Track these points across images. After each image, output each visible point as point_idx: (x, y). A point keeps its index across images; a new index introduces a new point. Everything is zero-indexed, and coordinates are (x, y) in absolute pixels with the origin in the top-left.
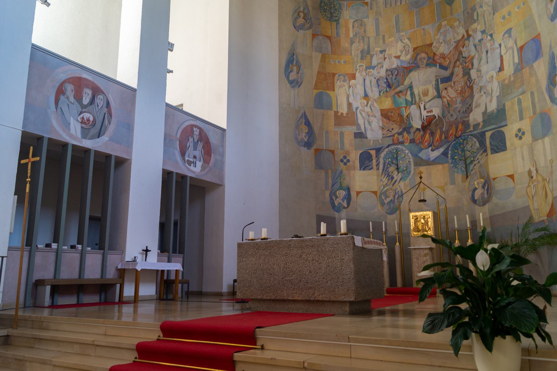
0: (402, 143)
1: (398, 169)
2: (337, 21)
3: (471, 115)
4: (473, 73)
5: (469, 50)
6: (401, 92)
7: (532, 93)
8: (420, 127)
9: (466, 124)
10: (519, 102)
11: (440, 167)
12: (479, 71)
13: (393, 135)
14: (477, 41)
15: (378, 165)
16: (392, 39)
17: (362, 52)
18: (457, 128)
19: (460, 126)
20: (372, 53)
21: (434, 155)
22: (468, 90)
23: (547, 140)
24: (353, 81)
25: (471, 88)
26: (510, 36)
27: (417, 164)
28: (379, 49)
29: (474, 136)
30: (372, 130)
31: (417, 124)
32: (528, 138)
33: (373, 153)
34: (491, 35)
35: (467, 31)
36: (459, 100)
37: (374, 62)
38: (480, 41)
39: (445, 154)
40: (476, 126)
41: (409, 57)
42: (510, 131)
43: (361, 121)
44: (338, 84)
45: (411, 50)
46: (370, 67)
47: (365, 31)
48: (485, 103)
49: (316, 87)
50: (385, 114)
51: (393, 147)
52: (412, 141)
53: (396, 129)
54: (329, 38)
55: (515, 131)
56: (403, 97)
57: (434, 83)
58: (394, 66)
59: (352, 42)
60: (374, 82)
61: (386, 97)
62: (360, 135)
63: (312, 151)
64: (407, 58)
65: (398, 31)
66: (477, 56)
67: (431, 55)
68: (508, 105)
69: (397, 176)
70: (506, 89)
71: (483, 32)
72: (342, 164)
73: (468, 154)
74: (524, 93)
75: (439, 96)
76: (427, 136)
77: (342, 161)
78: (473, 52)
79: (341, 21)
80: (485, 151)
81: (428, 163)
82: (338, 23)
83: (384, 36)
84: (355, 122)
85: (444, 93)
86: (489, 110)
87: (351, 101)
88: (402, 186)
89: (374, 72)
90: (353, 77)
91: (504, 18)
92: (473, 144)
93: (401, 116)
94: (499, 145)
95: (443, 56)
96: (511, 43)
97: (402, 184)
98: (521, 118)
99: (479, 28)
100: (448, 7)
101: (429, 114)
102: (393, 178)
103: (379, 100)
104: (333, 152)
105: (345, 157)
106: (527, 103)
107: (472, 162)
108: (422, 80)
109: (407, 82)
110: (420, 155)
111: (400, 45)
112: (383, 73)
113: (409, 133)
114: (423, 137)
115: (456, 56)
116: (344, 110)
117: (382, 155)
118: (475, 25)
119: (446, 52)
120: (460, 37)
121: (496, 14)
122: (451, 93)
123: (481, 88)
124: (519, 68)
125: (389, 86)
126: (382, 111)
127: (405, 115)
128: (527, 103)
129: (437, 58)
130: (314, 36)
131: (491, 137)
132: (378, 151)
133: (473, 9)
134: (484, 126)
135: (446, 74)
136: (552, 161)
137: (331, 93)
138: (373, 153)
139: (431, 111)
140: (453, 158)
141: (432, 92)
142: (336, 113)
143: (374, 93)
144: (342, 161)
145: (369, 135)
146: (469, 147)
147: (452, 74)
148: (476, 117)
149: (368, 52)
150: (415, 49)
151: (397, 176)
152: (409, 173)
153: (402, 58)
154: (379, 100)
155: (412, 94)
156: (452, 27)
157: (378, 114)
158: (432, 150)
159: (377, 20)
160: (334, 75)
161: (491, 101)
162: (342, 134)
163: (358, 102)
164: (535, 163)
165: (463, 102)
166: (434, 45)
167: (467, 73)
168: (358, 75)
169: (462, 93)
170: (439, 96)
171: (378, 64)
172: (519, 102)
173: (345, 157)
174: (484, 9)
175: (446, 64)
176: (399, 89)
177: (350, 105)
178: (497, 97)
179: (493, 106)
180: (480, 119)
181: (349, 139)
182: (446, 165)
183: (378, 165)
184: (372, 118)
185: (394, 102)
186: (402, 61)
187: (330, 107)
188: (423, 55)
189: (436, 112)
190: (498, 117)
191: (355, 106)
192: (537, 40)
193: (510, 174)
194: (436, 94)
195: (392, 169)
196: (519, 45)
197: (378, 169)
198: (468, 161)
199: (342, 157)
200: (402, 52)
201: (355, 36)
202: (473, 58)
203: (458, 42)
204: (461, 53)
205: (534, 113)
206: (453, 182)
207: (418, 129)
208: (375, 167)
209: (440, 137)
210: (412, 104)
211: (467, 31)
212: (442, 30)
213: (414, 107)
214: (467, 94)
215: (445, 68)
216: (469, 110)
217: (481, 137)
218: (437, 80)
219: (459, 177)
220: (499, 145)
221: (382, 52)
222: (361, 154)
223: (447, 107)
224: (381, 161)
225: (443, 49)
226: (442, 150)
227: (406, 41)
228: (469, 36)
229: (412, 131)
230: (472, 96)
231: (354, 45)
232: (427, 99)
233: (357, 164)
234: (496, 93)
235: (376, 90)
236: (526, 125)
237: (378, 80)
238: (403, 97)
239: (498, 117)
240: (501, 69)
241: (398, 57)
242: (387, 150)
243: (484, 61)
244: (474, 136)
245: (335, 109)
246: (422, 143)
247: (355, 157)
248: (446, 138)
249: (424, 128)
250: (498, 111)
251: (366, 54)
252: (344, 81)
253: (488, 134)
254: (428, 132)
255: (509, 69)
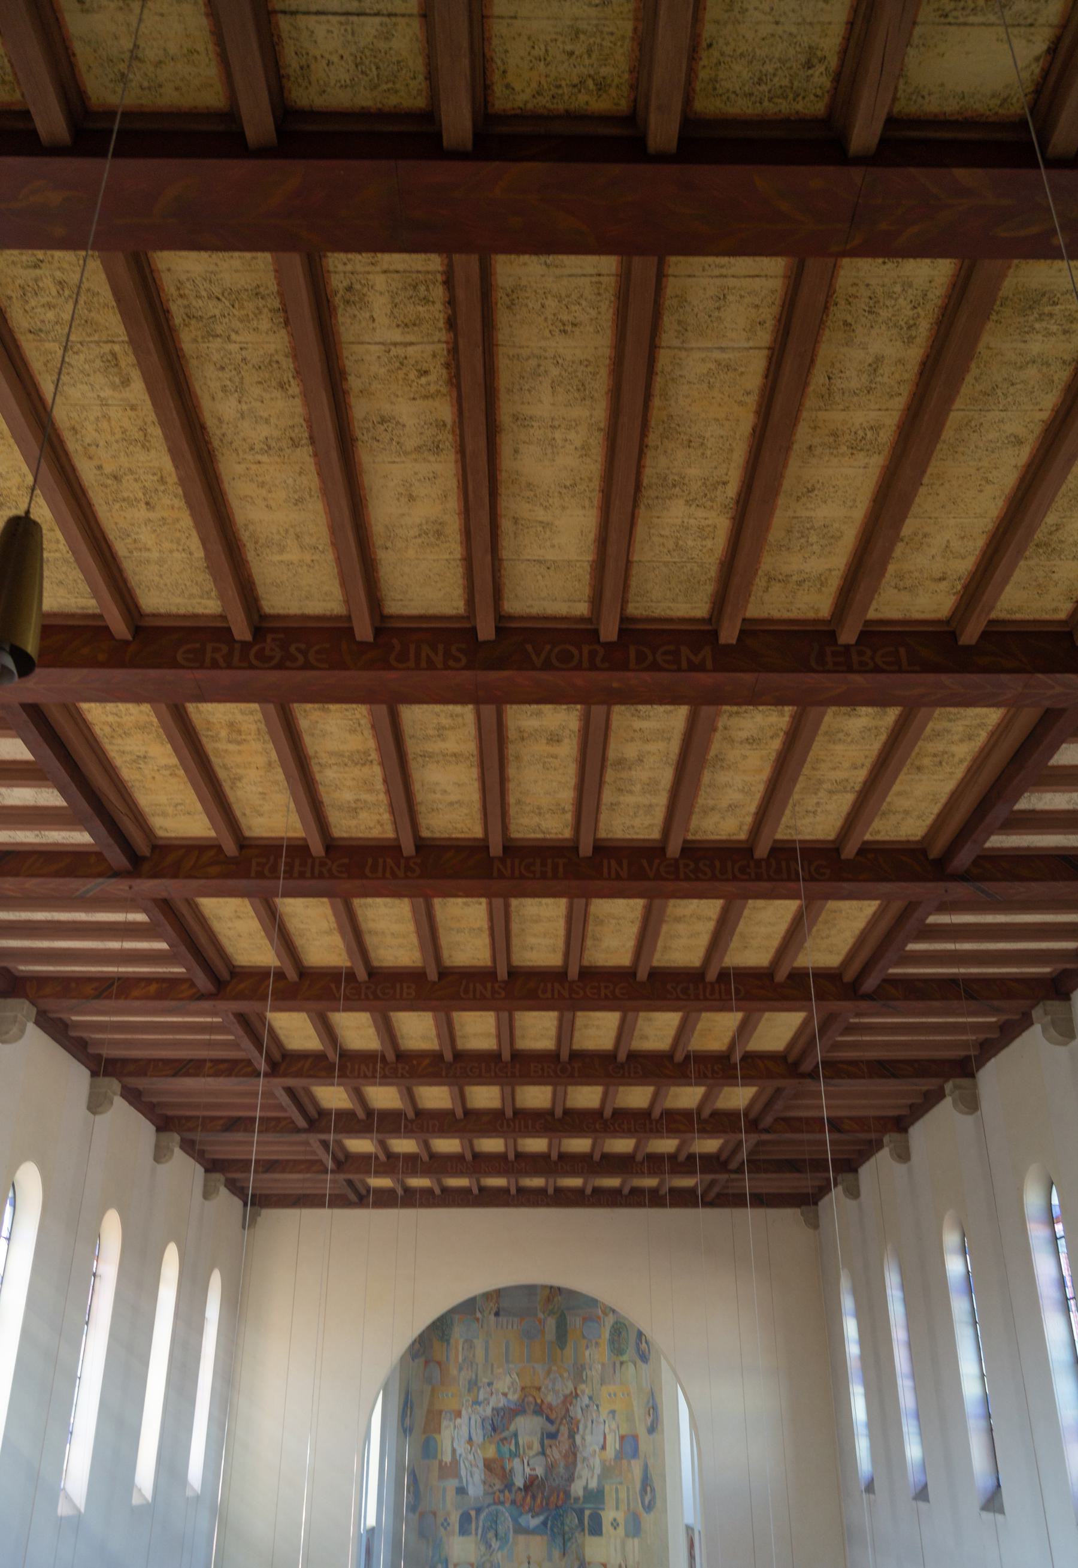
0: (502, 1503)
1: (496, 1535)
2: (448, 1341)
3: (573, 1486)
4: (578, 1438)
5: (576, 1412)
6: (506, 1439)
7: (628, 1488)
8: (521, 1486)
9: (567, 1494)
10: (617, 1491)
11: (538, 1538)
12: (583, 1438)
13: (494, 1493)
14: (584, 1406)
15: (477, 1529)
16: (501, 1370)
17: (470, 1382)
18: (558, 1496)
19: (561, 1494)
20: (479, 1384)
21: (534, 1522)
22: (572, 1455)
23: (636, 1541)
24: (458, 1421)
25: (575, 1455)
26: (614, 1418)
27: (516, 1532)
28: (486, 1380)
29: (574, 1510)
30: (474, 1484)
31: (519, 1482)
32: (621, 1530)
33: (473, 1513)
34: (597, 1406)
35: (576, 1389)
36: (562, 1464)
37: (481, 1397)
38: (587, 1406)
39: (544, 1523)
40: (577, 1499)
41: (516, 1397)
42: (608, 1515)
43: (463, 1473)
44: (444, 1423)
45: (519, 1389)
46: (476, 1402)
47: (474, 1356)
48: (586, 1479)
49: (424, 1432)
50: (488, 1465)
51: (493, 1507)
52: (513, 1502)
53: (498, 1486)
54: (439, 1363)
55: (611, 1519)
56: (507, 1445)
57: (539, 1435)
58: (501, 1405)
59: (461, 1369)
60: (479, 1420)
61: (490, 1443)
62: (461, 1491)
63: (417, 1514)
64: (514, 1397)
65: (507, 1361)
66: (582, 1422)
67: (539, 1401)
68: (607, 1488)
69: (495, 1544)
70: (607, 1471)
71: (590, 1398)
72: (442, 1529)
73: (567, 1528)
74: (621, 1483)
75: (543, 1453)
76: (529, 1498)
77: (442, 1525)
78: (579, 1415)
79: (452, 1341)
80: (583, 1530)
81: (527, 1531)
82: (448, 1344)
83: (492, 1365)
84: (457, 1475)
85: (548, 1452)
86: (590, 1486)
87: (455, 1446)
88: (499, 1556)
89: (480, 1409)
90: (459, 1414)
91: (610, 1395)
92: (572, 1520)
93: (503, 1468)
94: (596, 1529)
95: (550, 1407)
96: (614, 1426)
97: (499, 1555)
98: (617, 1508)
99: (587, 1391)
100: (559, 1351)
101: (533, 1473)
102: (490, 1546)
103: (482, 1447)
104: (435, 1514)
105: (446, 1520)
106: (623, 1495)
107: (570, 1539)
108: (528, 1428)
109: (512, 1428)
110: (520, 1520)
111: (508, 1380)
112: (489, 1412)
113: (510, 1491)
114: (524, 1499)
115: (563, 1412)
116: (447, 1458)
117: (482, 1516)
118: (583, 1386)
119: (554, 1403)
120: (567, 1392)
121: (604, 1387)
122: (555, 1454)
123: (584, 1459)
124: (620, 1455)
125: (494, 1429)
126: (485, 1460)
127: (508, 1468)
128: (623, 1495)
129: (544, 1407)
130: (427, 1363)
131: (591, 1516)
132: (478, 1511)
133: (583, 1367)
134: (584, 1502)
135: (552, 1429)
136: (638, 1563)
137: (436, 1436)
138: (473, 1513)
139: (534, 1469)
140: (552, 1530)
141: (537, 1447)
142: (441, 1462)
143: (478, 1438)
144: (442, 1525)
145: (471, 1491)
146: (568, 1521)
147: (558, 1431)
148: (577, 1489)
149: (476, 1383)
150: (523, 1389)
151: (495, 1544)
152: (507, 1542)
153: (510, 1396)
154: (482, 1447)
155: (517, 1444)
156: (561, 1376)
157: (481, 1464)
158: (533, 1517)
159: (487, 1342)
160: (441, 1412)
161: (592, 1477)
162: (444, 1490)
163: (461, 1448)
164: (625, 1559)
165: (567, 1467)
166: (543, 1389)
167: (572, 1436)
168: (464, 1412)
169: (566, 1456)
170: (543, 1453)
171: (485, 1399)
172: (617, 1491)
173: (446, 1520)
174: (594, 1373)
175: (553, 1416)
176: (506, 1434)
177: (454, 1451)
178: (599, 1476)
179: (593, 1484)
180: (581, 1493)
181: (451, 1494)
182: (545, 1538)
183: (477, 1529)
184: (475, 1469)
185: (499, 1450)
186: (509, 1401)
187: (435, 1457)
188: (531, 1399)
189: (540, 1471)
190: (596, 1497)
191: (458, 1452)
192: (635, 1438)
193: (603, 1561)
194: (540, 1449)
195: (490, 1534)
196: (622, 1432)
197: (476, 1534)
198: (566, 1537)
199: (442, 1520)
200: (509, 1389)
201: (464, 1360)
202: (578, 1422)
203: (566, 1397)
204: (568, 1410)
205: (628, 1509)
206: (550, 1559)
207: (520, 1489)
208: (473, 1532)
209: (542, 1502)
210: (516, 1455)
211: (576, 1389)
212: (552, 1376)
213: (516, 1462)
214: (570, 1460)
215: (552, 1422)
216: (571, 1479)
217: (580, 1513)
218: (542, 1434)
219: (556, 1554)
220: (596, 1529)
221: (490, 1384)
222: (462, 1516)
223: (550, 1468)
224: (481, 1524)
225: (550, 1399)
226: (541, 1518)
227: (515, 1376)
228: (577, 1395)
229: (514, 1489)
230: (574, 1464)
231: (463, 1373)
232: (532, 1453)
233: (457, 1530)
234: (598, 1471)
235: (480, 1432)
236: (620, 1516)
237: (483, 1420)
238: (507, 1445)
239: (596, 1497)
240: (604, 1448)
241: (505, 1395)
242: (486, 1511)
243: (588, 1431)
244: (574, 1510)
245: (439, 1457)
246: (522, 1505)
247: (455, 1518)
248: (547, 1504)
249: (527, 1487)
250: (598, 1491)
251: (473, 1385)
252: (451, 1420)
253: (587, 1513)
254: (530, 1494)
255: (610, 1452)
